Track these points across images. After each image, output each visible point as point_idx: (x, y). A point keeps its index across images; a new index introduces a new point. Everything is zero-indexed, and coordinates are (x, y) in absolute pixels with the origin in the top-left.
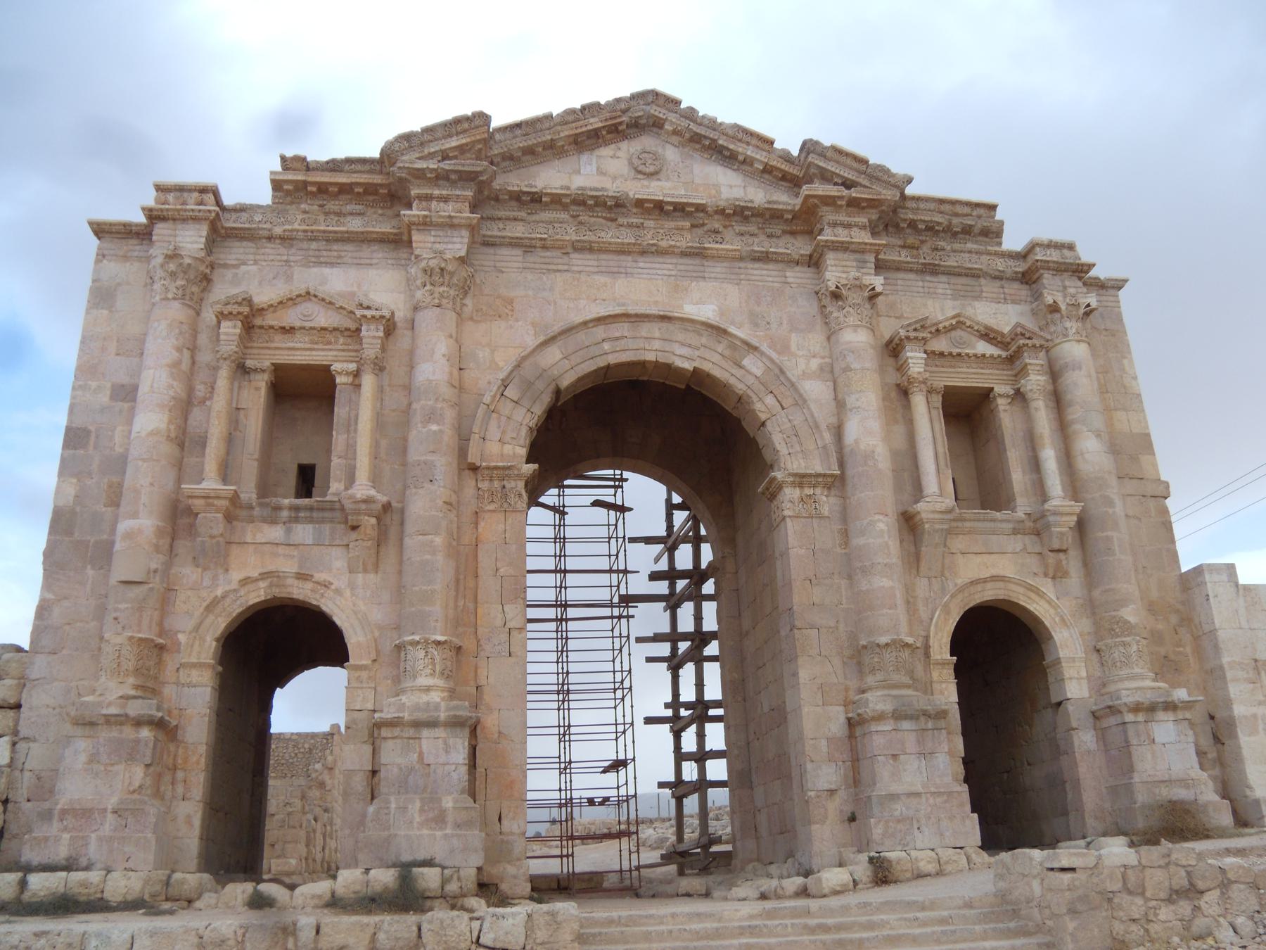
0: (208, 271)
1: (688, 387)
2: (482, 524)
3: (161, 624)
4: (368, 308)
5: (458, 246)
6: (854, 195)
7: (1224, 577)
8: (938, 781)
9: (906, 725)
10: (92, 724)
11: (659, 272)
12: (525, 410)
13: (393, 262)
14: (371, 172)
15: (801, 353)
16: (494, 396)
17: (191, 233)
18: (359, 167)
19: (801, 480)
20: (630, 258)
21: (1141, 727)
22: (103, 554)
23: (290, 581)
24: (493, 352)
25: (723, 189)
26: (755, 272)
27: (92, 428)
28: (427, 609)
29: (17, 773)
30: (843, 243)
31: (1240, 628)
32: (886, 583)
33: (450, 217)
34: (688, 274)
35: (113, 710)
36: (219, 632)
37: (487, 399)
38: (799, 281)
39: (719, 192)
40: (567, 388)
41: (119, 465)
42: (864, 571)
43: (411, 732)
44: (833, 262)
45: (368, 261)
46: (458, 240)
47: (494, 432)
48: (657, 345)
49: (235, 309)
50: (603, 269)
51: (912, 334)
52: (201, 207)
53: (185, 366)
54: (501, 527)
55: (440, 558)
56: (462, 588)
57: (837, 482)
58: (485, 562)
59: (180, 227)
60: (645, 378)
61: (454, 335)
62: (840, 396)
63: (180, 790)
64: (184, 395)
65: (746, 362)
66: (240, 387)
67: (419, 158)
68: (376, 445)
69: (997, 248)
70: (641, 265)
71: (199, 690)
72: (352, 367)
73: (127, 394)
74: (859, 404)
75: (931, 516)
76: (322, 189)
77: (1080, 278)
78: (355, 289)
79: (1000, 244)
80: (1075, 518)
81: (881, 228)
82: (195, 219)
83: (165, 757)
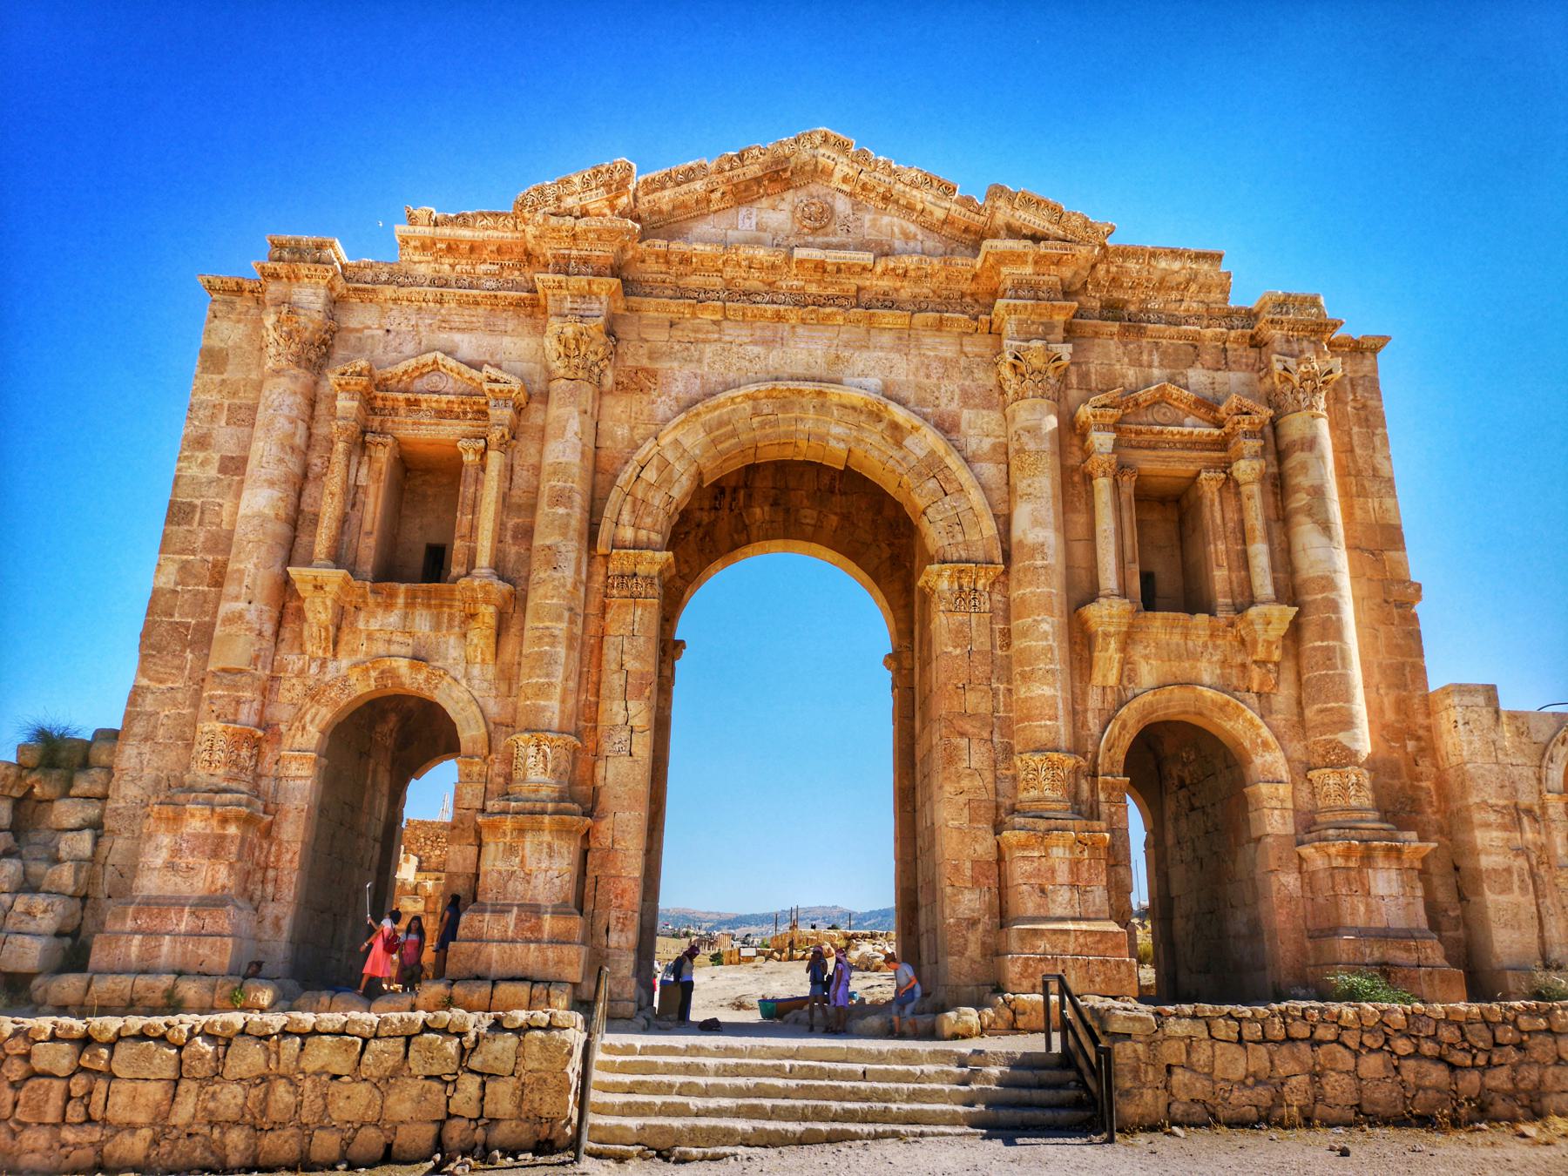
0: (328, 337)
2: (608, 617)
3: (261, 713)
4: (496, 381)
7: (1481, 700)
12: (662, 493)
15: (972, 432)
16: (631, 477)
21: (1353, 873)
22: (203, 638)
24: (632, 429)
27: (198, 502)
28: (542, 703)
29: (99, 868)
32: (1047, 691)
36: (324, 723)
37: (621, 481)
41: (223, 542)
42: (1023, 676)
46: (597, 306)
47: (626, 517)
53: (299, 440)
54: (629, 618)
55: (561, 650)
56: (585, 682)
58: (611, 654)
60: (801, 459)
61: (589, 411)
62: (1012, 482)
63: (270, 889)
64: (297, 470)
65: (908, 442)
66: (359, 463)
68: (501, 527)
69: (1222, 306)
71: (298, 782)
73: (235, 466)
74: (1030, 490)
76: (452, 248)
79: (1226, 300)
81: (1078, 286)
83: (257, 854)
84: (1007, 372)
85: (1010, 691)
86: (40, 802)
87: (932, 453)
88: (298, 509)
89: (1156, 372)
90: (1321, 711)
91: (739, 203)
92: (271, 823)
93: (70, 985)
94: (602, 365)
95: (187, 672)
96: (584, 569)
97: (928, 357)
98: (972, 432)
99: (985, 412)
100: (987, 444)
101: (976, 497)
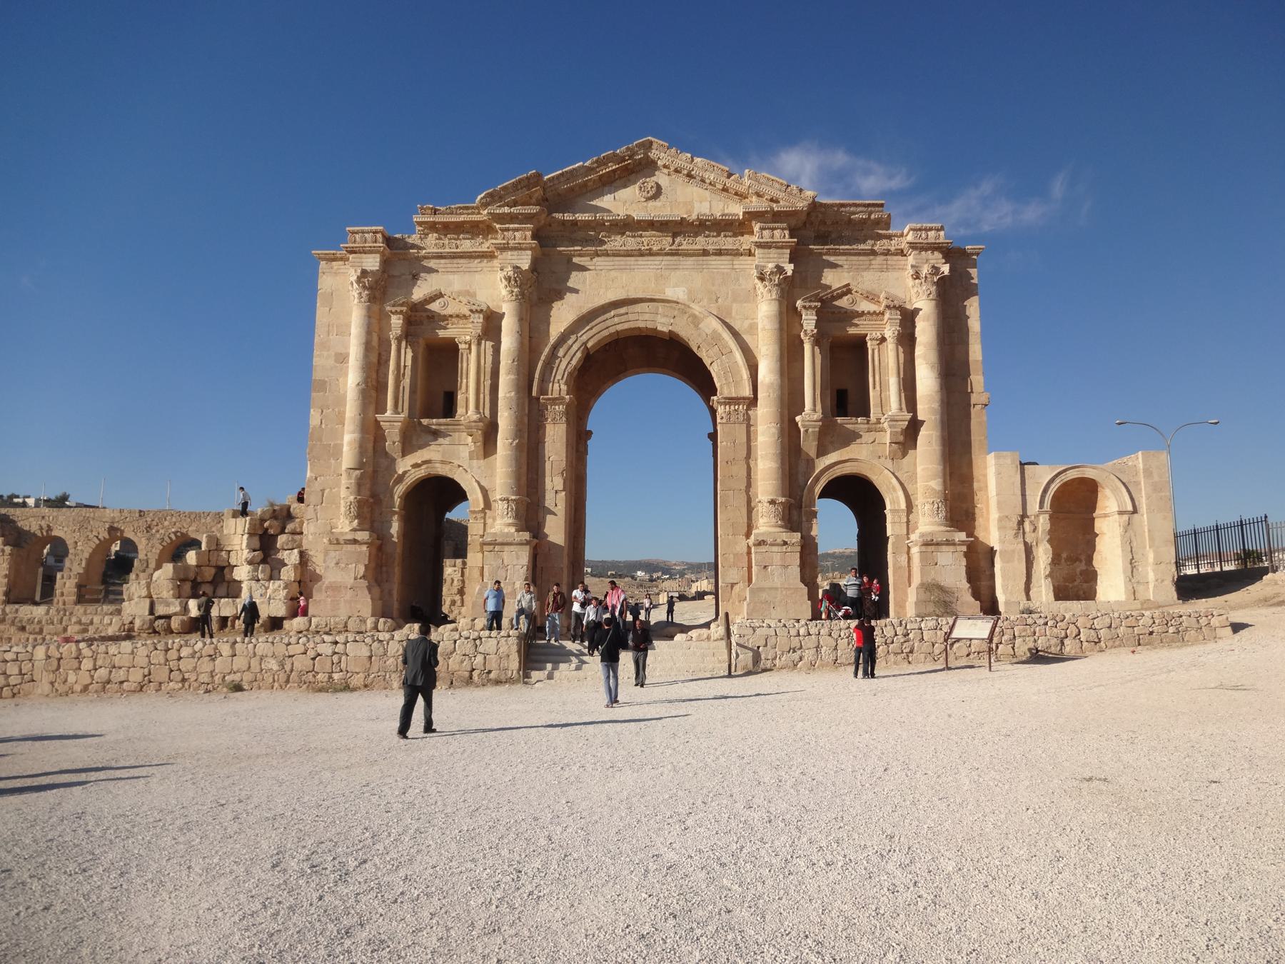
1: (671, 338)
5: (526, 261)
6: (776, 209)
8: (791, 581)
9: (775, 549)
10: (338, 543)
11: (652, 267)
13: (489, 269)
14: (473, 213)
15: (738, 317)
17: (371, 260)
18: (465, 211)
19: (731, 401)
20: (633, 258)
23: (437, 465)
25: (696, 205)
26: (713, 263)
30: (767, 242)
31: (1014, 495)
33: (520, 244)
34: (670, 267)
35: (350, 537)
37: (543, 358)
38: (741, 267)
39: (693, 207)
40: (592, 346)
43: (497, 548)
44: (761, 256)
45: (475, 270)
46: (525, 257)
48: (647, 317)
49: (399, 309)
50: (616, 267)
51: (807, 304)
52: (375, 245)
57: (753, 402)
59: (364, 255)
64: (375, 360)
67: (499, 206)
70: (640, 263)
72: (468, 338)
75: (807, 423)
77: (942, 252)
78: (468, 288)
80: (907, 423)
82: (371, 252)
84: (757, 281)
85: (756, 464)
86: (272, 535)
87: (714, 331)
88: (378, 382)
89: (846, 274)
90: (923, 469)
91: (604, 185)
92: (381, 545)
93: (299, 622)
94: (530, 290)
95: (332, 470)
96: (527, 408)
97: (713, 273)
98: (738, 317)
99: (745, 305)
100: (747, 323)
101: (738, 356)
